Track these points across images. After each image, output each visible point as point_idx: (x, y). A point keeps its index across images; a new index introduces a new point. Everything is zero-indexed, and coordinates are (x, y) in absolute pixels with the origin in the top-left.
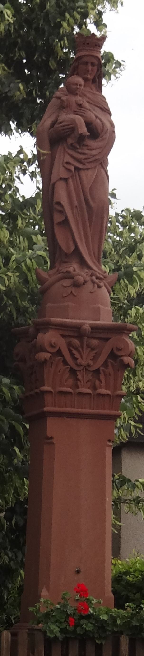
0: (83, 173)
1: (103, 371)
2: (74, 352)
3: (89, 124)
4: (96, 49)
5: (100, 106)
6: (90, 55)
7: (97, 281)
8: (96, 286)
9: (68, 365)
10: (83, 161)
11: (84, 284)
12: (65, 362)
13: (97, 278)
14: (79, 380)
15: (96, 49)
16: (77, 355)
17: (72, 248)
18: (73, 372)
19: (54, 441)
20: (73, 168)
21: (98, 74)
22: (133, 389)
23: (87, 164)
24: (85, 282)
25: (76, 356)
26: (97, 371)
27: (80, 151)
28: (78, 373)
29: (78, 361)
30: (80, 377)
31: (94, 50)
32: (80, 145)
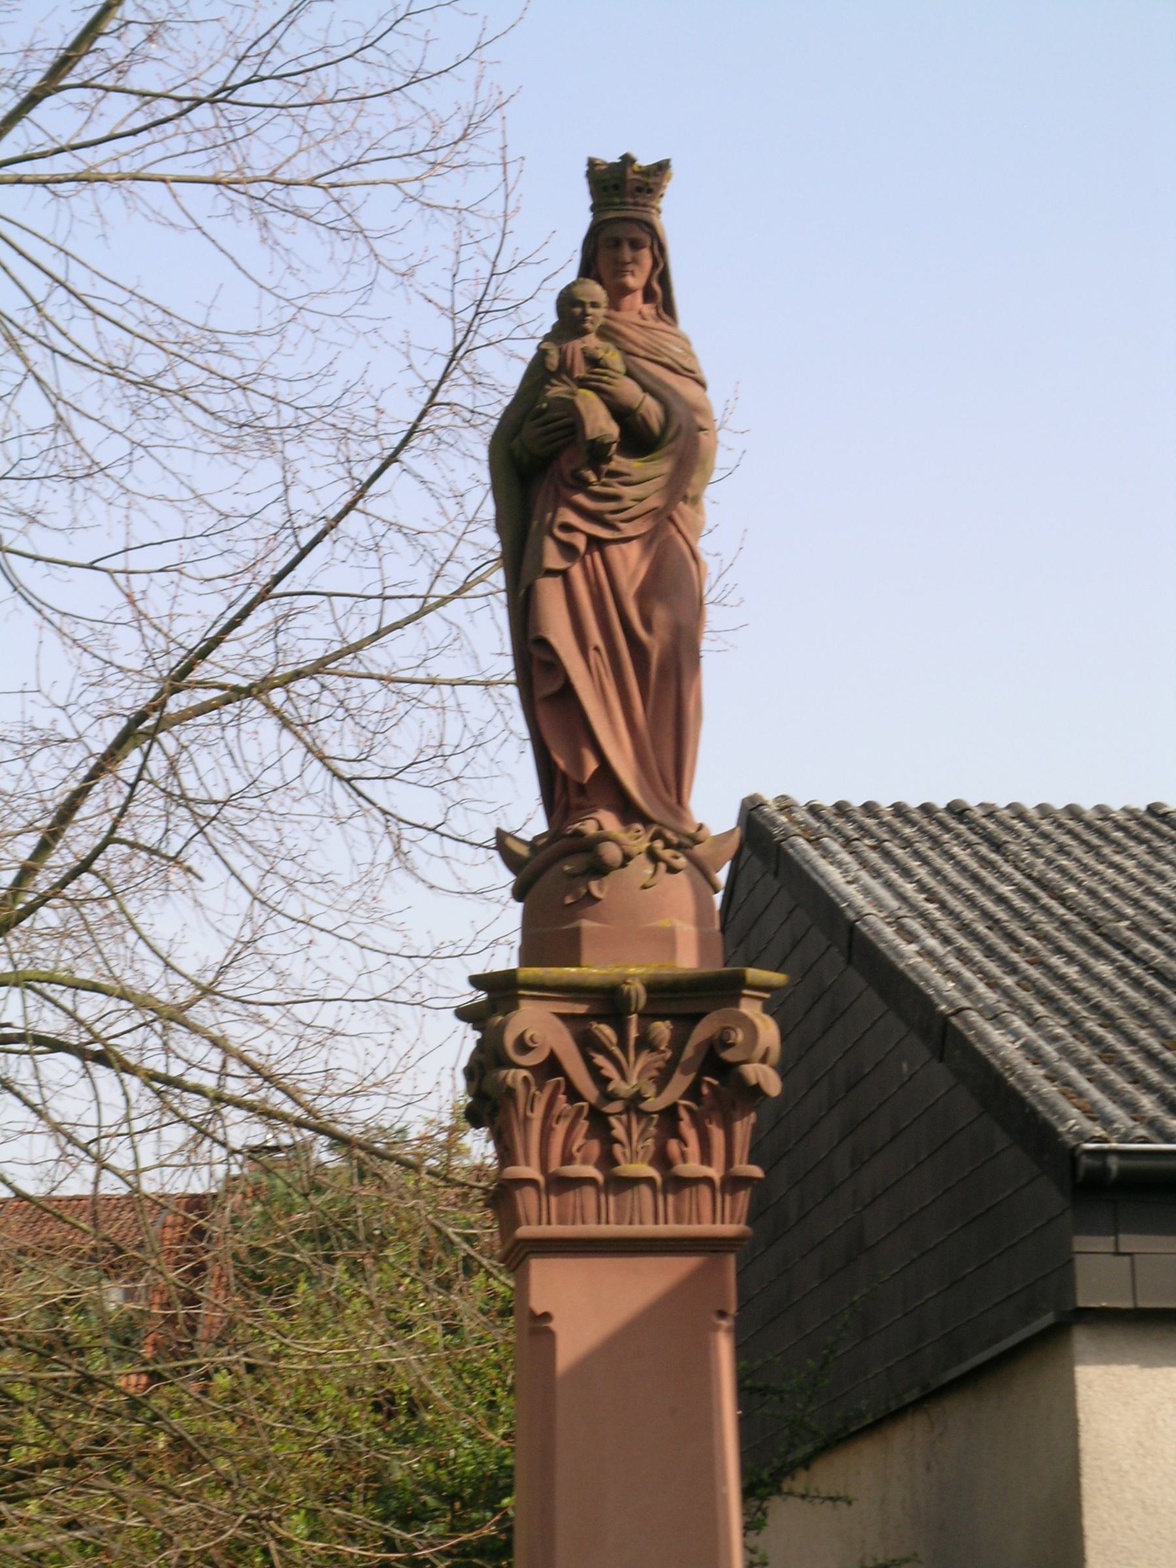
0: (613, 551)
1: (687, 1108)
2: (600, 1060)
3: (621, 413)
4: (641, 200)
5: (666, 360)
6: (625, 219)
7: (667, 854)
8: (662, 866)
9: (582, 1099)
10: (609, 517)
11: (623, 865)
12: (574, 1095)
13: (668, 845)
14: (617, 1141)
15: (641, 200)
16: (609, 1070)
17: (591, 765)
18: (599, 1123)
19: (553, 1325)
20: (580, 542)
21: (658, 272)
22: (283, 964)
23: (622, 525)
24: (627, 858)
25: (604, 1072)
26: (670, 1114)
27: (597, 488)
28: (613, 1121)
29: (611, 1087)
30: (619, 1131)
31: (636, 204)
32: (598, 473)
